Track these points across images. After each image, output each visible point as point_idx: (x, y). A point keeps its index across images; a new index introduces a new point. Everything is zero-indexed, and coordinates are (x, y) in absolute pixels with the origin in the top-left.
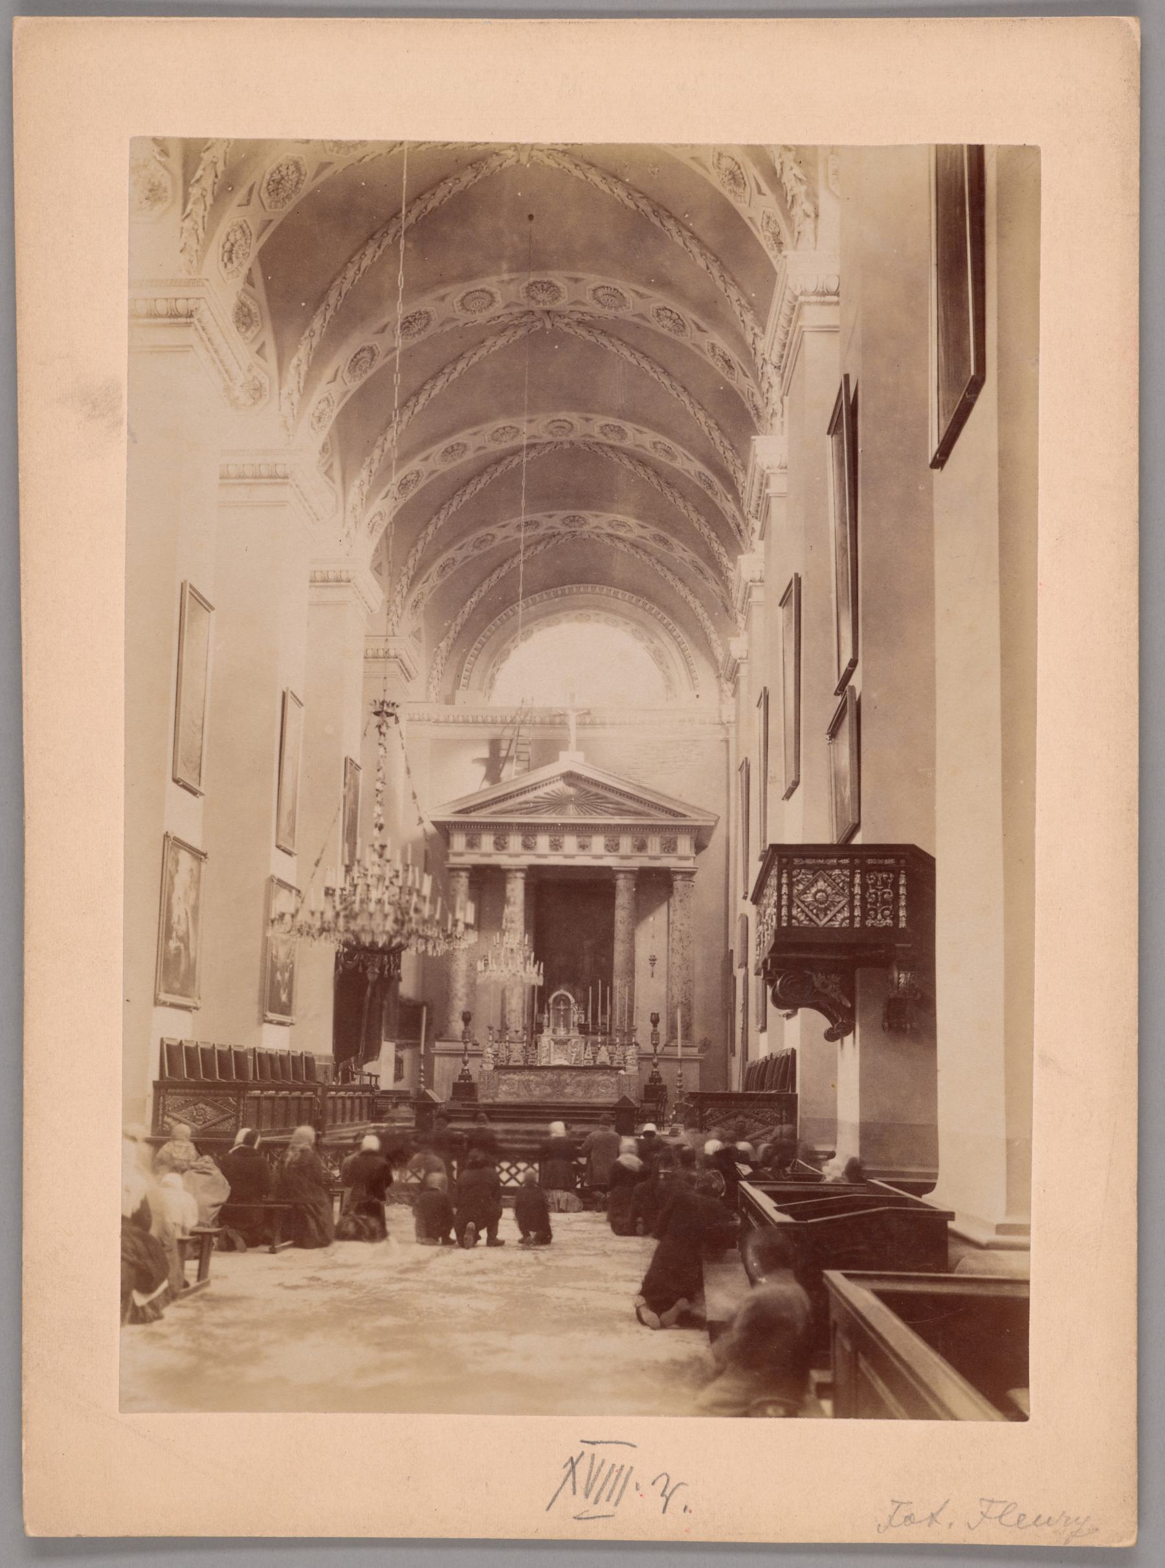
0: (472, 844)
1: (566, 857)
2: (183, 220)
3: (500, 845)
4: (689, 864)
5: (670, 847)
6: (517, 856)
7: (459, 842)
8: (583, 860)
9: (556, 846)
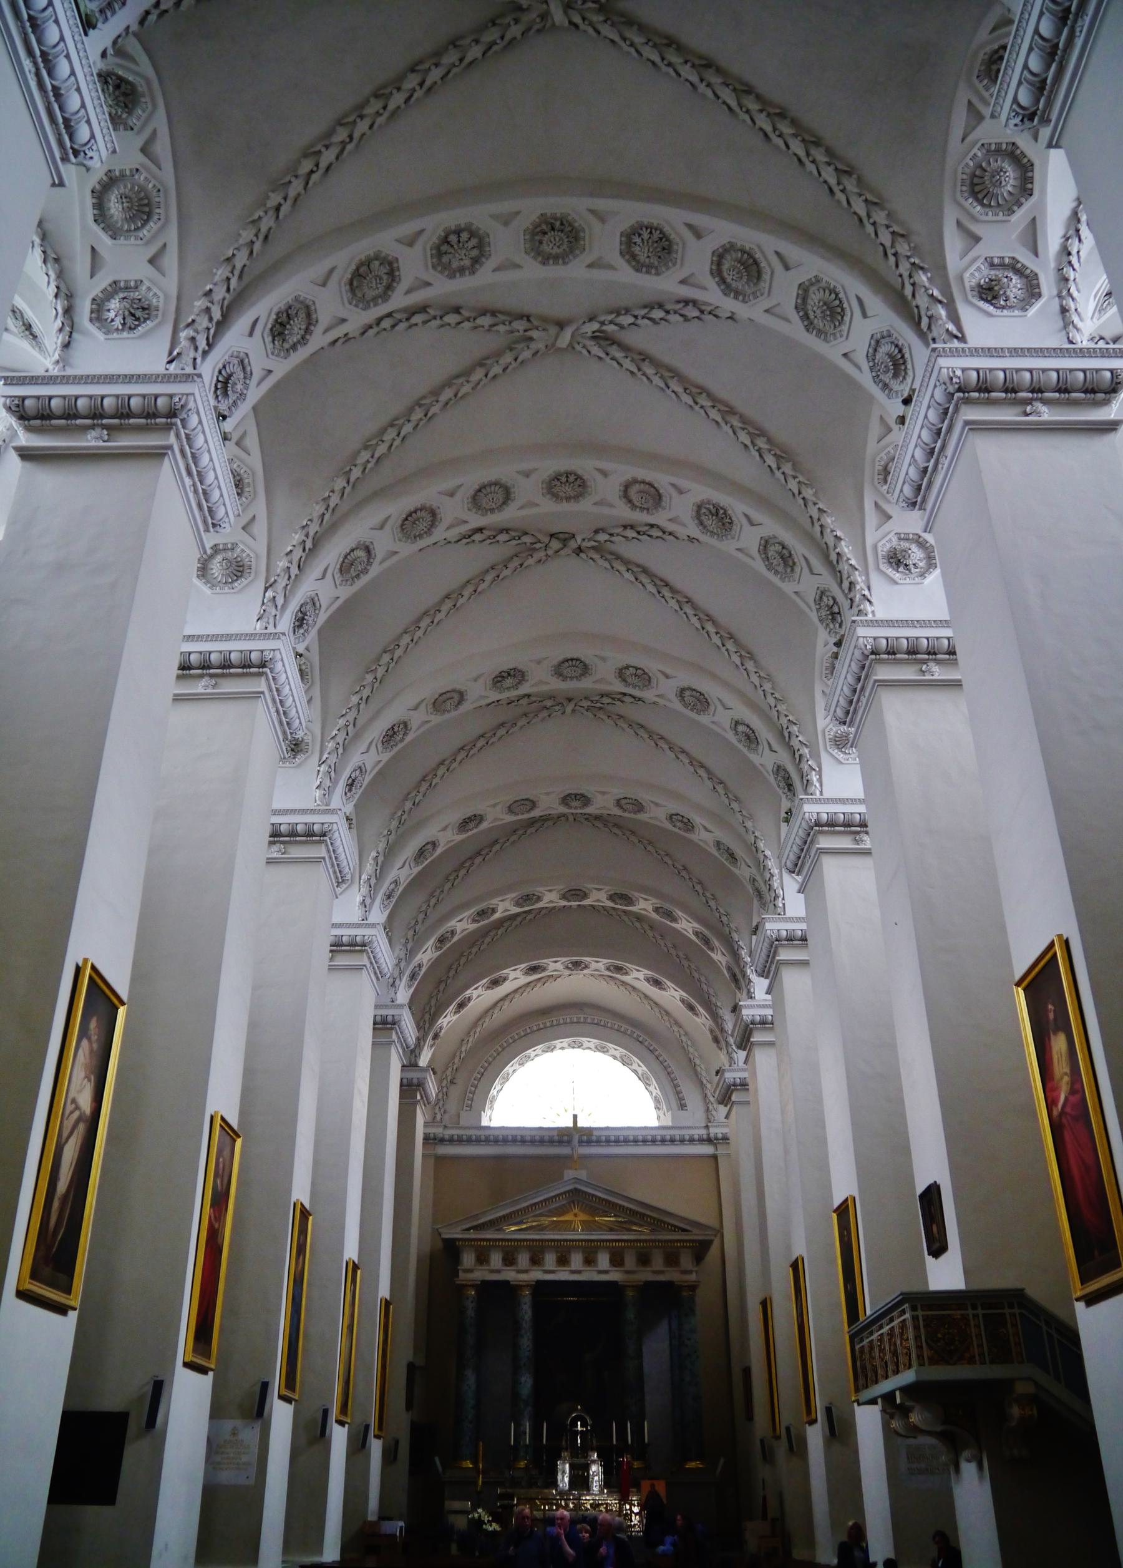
0: (482, 1259)
1: (573, 1272)
2: (320, 766)
3: (509, 1260)
4: (693, 1277)
5: (672, 1260)
6: (526, 1271)
7: (468, 1259)
8: (589, 1275)
9: (563, 1261)
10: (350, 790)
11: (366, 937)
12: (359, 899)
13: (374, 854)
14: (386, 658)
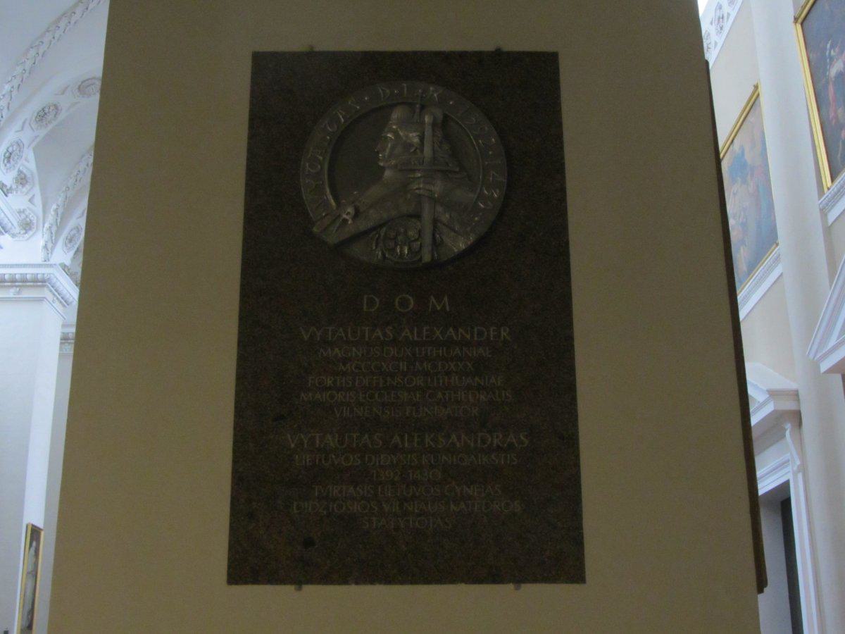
10: (9, 162)
11: (46, 276)
12: (42, 243)
13: (54, 207)
14: (32, 53)
